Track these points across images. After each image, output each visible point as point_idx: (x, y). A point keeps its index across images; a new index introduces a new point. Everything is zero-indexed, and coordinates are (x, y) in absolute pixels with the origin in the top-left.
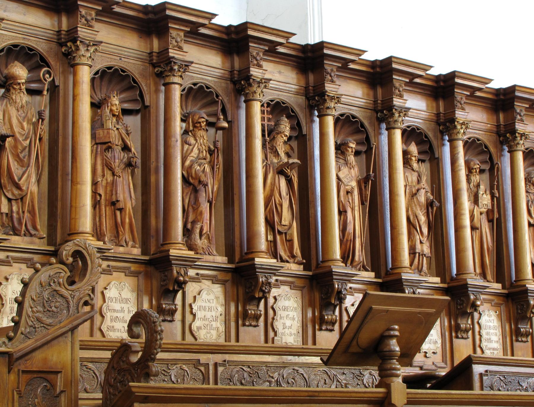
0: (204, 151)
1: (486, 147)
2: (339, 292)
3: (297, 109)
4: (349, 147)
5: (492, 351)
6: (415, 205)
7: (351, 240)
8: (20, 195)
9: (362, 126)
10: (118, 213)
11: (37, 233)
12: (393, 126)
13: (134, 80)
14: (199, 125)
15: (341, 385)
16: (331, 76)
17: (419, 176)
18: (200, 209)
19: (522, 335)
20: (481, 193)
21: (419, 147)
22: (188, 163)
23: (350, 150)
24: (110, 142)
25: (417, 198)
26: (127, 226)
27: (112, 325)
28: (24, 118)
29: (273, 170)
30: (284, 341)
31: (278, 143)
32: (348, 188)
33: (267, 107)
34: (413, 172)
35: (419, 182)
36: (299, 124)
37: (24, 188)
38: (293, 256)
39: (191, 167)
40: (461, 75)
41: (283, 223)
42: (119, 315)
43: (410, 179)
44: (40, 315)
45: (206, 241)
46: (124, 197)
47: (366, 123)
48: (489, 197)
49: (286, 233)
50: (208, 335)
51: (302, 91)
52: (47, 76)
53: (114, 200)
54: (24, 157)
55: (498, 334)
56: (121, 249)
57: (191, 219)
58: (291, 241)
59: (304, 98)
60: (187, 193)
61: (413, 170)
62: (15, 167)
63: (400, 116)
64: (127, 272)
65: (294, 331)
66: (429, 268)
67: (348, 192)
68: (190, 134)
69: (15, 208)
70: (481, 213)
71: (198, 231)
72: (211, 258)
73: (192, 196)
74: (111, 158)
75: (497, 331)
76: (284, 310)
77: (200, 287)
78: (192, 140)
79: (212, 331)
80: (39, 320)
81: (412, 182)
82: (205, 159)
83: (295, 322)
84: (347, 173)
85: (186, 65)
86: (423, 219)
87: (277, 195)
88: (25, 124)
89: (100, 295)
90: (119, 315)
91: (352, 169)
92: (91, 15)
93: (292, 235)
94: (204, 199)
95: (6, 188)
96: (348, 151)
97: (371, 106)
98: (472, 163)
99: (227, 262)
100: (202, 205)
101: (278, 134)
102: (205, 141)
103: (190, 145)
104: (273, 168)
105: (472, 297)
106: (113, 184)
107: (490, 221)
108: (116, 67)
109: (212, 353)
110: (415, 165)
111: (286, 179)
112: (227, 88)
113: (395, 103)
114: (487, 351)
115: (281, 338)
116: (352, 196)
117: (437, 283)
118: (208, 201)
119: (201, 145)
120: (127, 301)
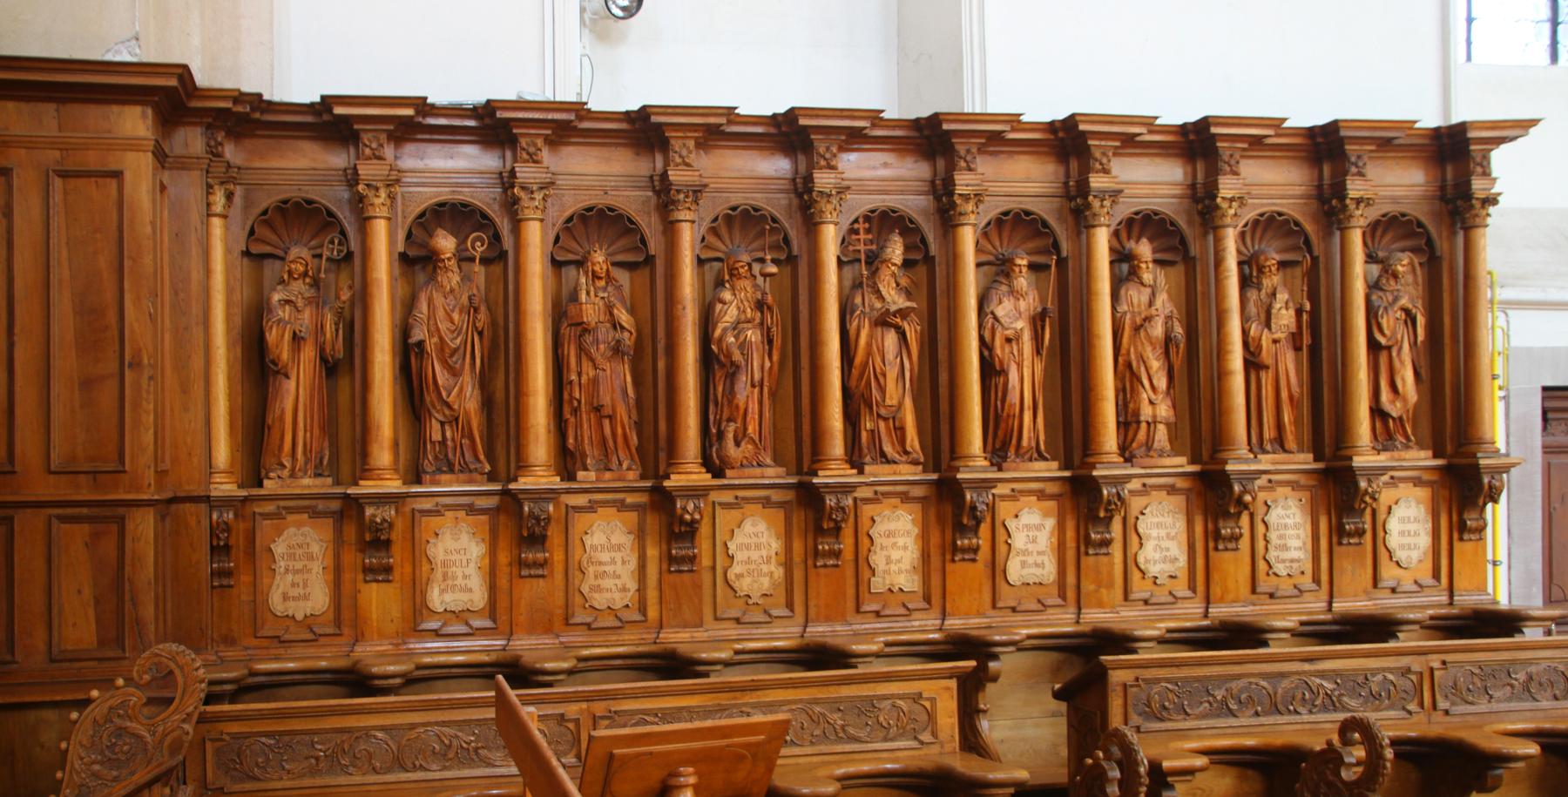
0: (749, 310)
1: (1297, 224)
2: (973, 508)
3: (920, 220)
4: (1015, 265)
5: (1288, 564)
6: (1143, 344)
7: (1014, 416)
8: (452, 416)
9: (1045, 224)
10: (606, 422)
11: (478, 466)
12: (1092, 222)
13: (630, 220)
14: (736, 272)
15: (835, 728)
16: (966, 161)
17: (1153, 294)
18: (736, 401)
19: (1350, 535)
20: (1278, 306)
21: (1155, 244)
22: (718, 333)
23: (1017, 269)
24: (583, 323)
25: (1146, 331)
26: (620, 439)
27: (596, 583)
28: (454, 307)
29: (870, 323)
30: (888, 582)
31: (882, 277)
32: (1009, 332)
33: (864, 223)
34: (1142, 289)
35: (1151, 304)
36: (923, 240)
37: (456, 407)
38: (906, 453)
39: (720, 340)
40: (1221, 120)
41: (888, 402)
42: (607, 568)
43: (1135, 301)
44: (96, 767)
45: (750, 447)
46: (612, 400)
47: (1052, 222)
48: (1292, 312)
49: (894, 418)
50: (756, 585)
51: (926, 189)
52: (479, 244)
53: (595, 405)
54: (456, 363)
55: (1302, 535)
56: (608, 475)
57: (725, 416)
58: (900, 431)
59: (931, 197)
60: (721, 377)
61: (1142, 284)
62: (442, 377)
63: (1102, 206)
64: (619, 505)
65: (906, 564)
66: (1173, 438)
67: (1009, 340)
68: (727, 285)
69: (449, 434)
70: (1275, 341)
71: (730, 436)
72: (758, 471)
73: (728, 381)
74: (592, 343)
75: (1301, 532)
76: (888, 536)
77: (743, 514)
78: (727, 296)
79: (762, 579)
80: (96, 775)
81: (1139, 305)
82: (749, 322)
83: (909, 553)
84: (1012, 307)
85: (697, 192)
86: (1156, 364)
87: (878, 360)
88: (456, 316)
89: (578, 542)
90: (607, 568)
91: (1021, 299)
92: (535, 145)
93: (903, 421)
94: (743, 386)
95: (434, 407)
96: (1013, 271)
97: (1060, 191)
98: (1262, 258)
99: (784, 475)
100: (738, 396)
101: (882, 262)
102: (748, 295)
103: (725, 303)
104: (870, 319)
105: (1237, 488)
106: (595, 382)
107: (1297, 348)
108: (600, 206)
109: (587, 701)
110: (1147, 277)
111: (897, 332)
112: (790, 205)
113: (1092, 185)
114: (1281, 566)
115: (884, 578)
116: (1018, 344)
117: (1182, 466)
118: (753, 386)
119: (742, 302)
120: (619, 547)
